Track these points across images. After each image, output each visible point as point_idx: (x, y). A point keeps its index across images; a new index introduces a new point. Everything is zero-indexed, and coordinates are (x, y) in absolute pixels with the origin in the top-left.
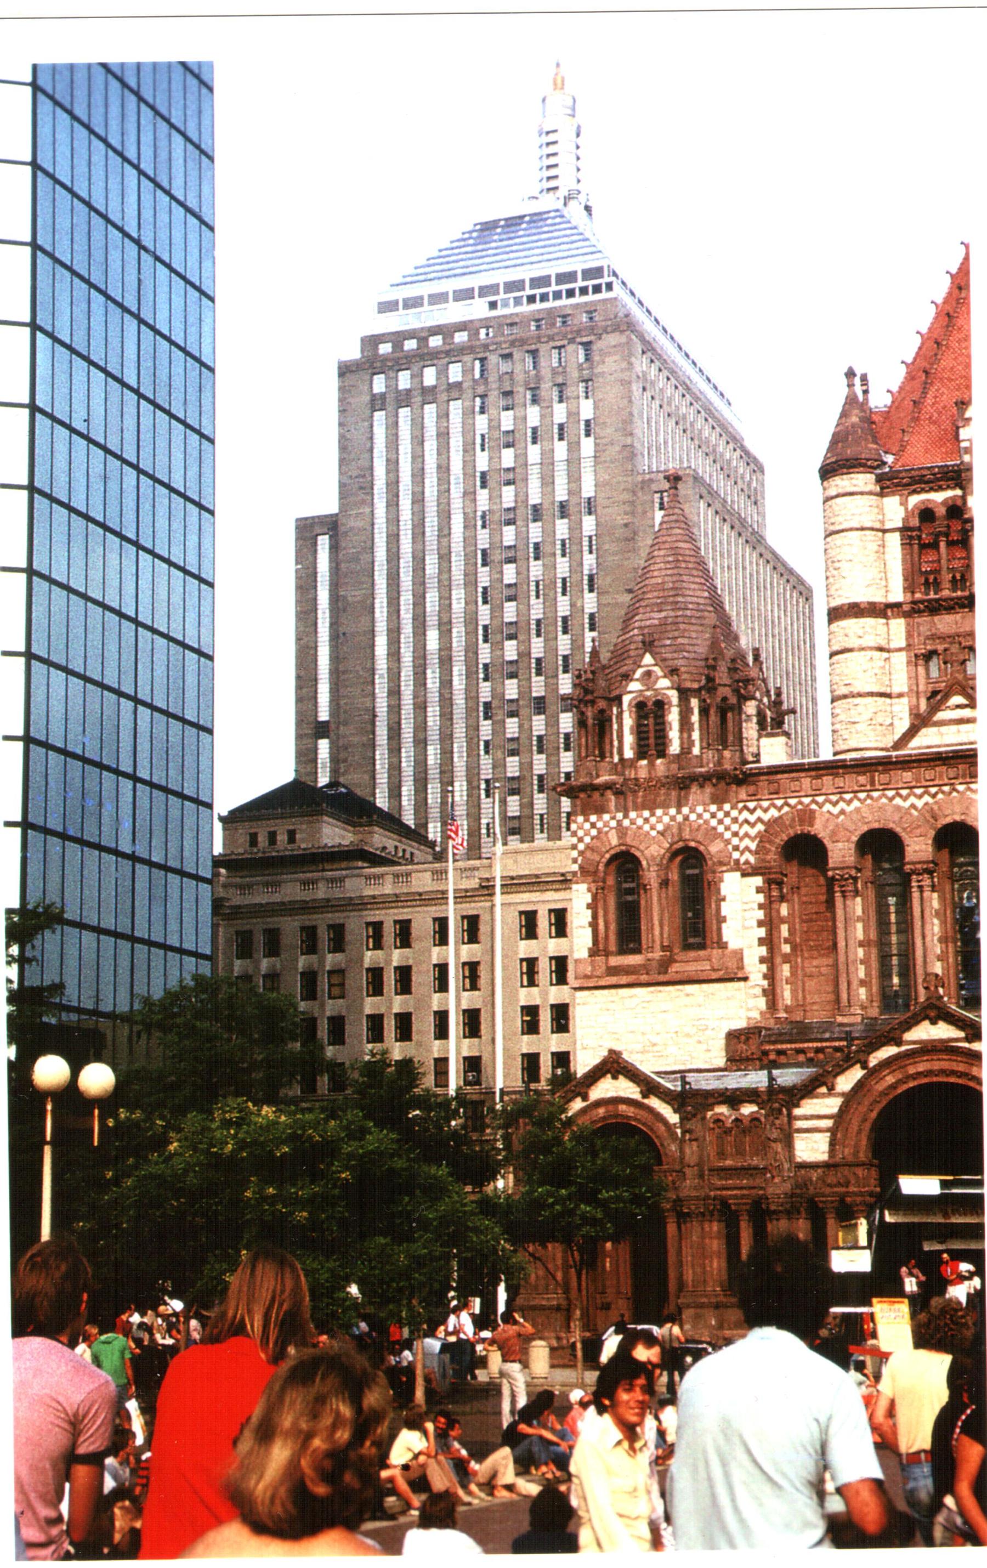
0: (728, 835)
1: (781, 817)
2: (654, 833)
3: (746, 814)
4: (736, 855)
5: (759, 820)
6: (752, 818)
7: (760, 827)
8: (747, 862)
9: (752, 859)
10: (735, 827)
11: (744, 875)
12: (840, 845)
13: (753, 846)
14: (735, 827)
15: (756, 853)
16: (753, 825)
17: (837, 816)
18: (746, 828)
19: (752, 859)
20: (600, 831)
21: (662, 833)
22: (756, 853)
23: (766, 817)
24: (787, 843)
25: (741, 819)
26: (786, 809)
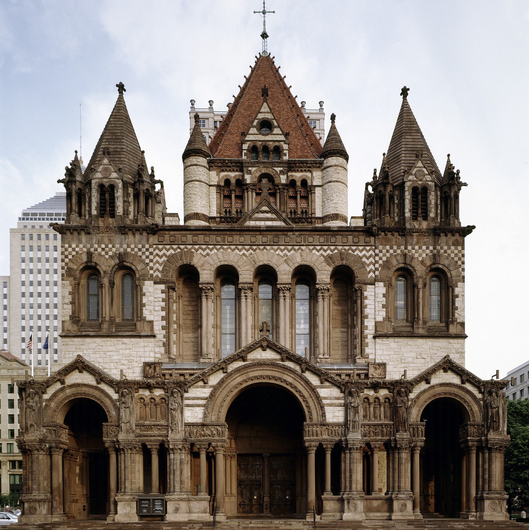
0: (147, 261)
1: (175, 254)
2: (107, 256)
3: (157, 251)
4: (151, 272)
5: (164, 254)
6: (161, 254)
7: (164, 258)
8: (157, 276)
9: (160, 275)
10: (151, 257)
11: (155, 283)
12: (206, 272)
13: (161, 268)
14: (151, 257)
15: (162, 272)
16: (161, 257)
17: (205, 256)
18: (157, 258)
19: (160, 275)
20: (77, 252)
21: (111, 257)
22: (162, 272)
23: (168, 253)
24: (180, 266)
25: (155, 253)
26: (179, 250)
